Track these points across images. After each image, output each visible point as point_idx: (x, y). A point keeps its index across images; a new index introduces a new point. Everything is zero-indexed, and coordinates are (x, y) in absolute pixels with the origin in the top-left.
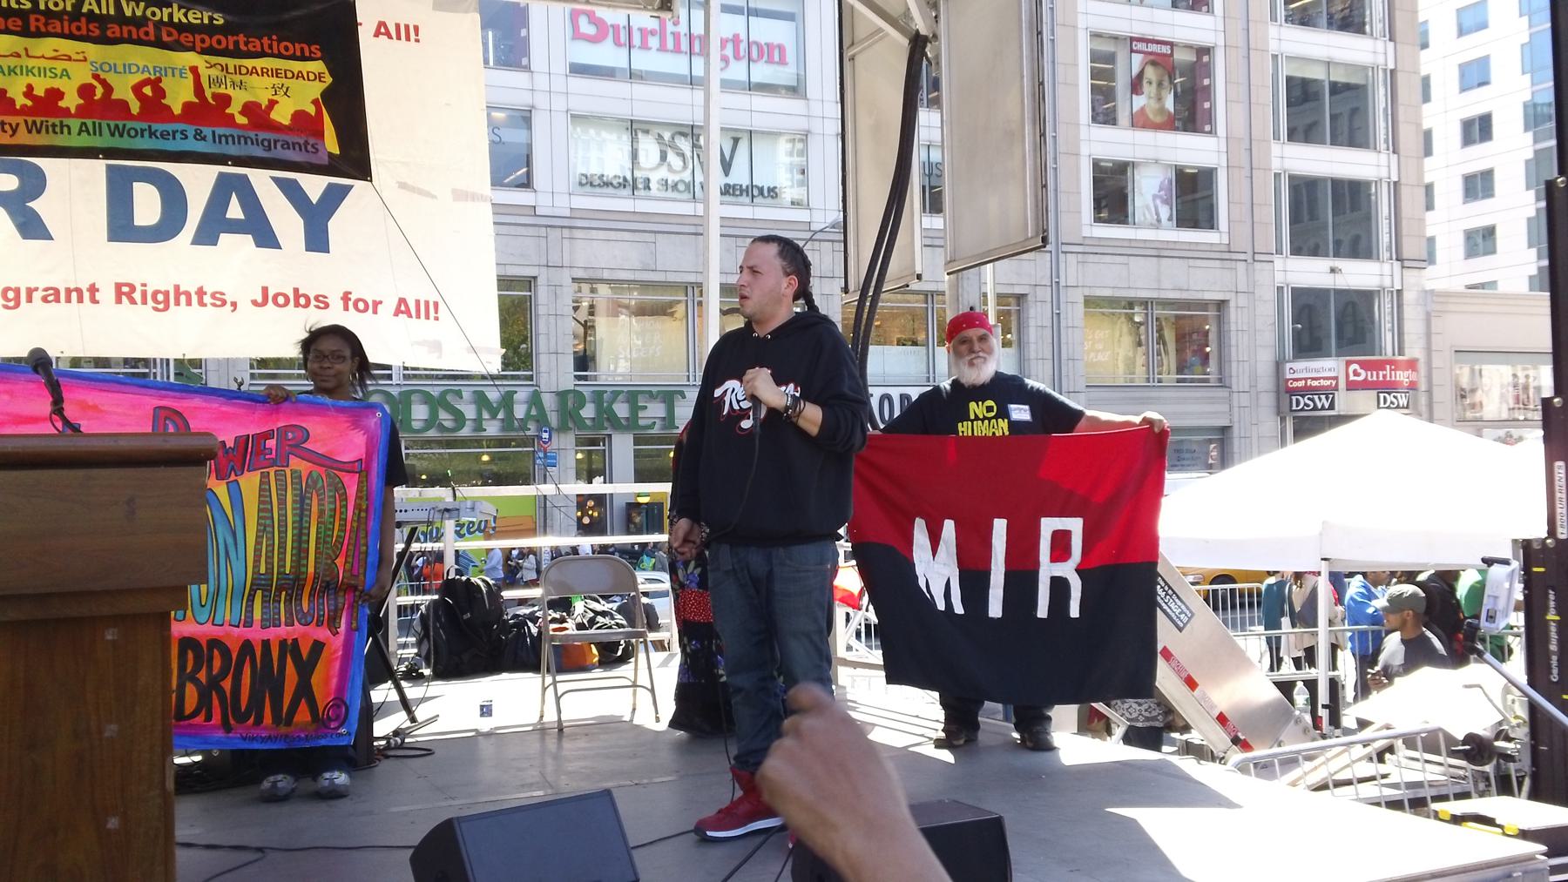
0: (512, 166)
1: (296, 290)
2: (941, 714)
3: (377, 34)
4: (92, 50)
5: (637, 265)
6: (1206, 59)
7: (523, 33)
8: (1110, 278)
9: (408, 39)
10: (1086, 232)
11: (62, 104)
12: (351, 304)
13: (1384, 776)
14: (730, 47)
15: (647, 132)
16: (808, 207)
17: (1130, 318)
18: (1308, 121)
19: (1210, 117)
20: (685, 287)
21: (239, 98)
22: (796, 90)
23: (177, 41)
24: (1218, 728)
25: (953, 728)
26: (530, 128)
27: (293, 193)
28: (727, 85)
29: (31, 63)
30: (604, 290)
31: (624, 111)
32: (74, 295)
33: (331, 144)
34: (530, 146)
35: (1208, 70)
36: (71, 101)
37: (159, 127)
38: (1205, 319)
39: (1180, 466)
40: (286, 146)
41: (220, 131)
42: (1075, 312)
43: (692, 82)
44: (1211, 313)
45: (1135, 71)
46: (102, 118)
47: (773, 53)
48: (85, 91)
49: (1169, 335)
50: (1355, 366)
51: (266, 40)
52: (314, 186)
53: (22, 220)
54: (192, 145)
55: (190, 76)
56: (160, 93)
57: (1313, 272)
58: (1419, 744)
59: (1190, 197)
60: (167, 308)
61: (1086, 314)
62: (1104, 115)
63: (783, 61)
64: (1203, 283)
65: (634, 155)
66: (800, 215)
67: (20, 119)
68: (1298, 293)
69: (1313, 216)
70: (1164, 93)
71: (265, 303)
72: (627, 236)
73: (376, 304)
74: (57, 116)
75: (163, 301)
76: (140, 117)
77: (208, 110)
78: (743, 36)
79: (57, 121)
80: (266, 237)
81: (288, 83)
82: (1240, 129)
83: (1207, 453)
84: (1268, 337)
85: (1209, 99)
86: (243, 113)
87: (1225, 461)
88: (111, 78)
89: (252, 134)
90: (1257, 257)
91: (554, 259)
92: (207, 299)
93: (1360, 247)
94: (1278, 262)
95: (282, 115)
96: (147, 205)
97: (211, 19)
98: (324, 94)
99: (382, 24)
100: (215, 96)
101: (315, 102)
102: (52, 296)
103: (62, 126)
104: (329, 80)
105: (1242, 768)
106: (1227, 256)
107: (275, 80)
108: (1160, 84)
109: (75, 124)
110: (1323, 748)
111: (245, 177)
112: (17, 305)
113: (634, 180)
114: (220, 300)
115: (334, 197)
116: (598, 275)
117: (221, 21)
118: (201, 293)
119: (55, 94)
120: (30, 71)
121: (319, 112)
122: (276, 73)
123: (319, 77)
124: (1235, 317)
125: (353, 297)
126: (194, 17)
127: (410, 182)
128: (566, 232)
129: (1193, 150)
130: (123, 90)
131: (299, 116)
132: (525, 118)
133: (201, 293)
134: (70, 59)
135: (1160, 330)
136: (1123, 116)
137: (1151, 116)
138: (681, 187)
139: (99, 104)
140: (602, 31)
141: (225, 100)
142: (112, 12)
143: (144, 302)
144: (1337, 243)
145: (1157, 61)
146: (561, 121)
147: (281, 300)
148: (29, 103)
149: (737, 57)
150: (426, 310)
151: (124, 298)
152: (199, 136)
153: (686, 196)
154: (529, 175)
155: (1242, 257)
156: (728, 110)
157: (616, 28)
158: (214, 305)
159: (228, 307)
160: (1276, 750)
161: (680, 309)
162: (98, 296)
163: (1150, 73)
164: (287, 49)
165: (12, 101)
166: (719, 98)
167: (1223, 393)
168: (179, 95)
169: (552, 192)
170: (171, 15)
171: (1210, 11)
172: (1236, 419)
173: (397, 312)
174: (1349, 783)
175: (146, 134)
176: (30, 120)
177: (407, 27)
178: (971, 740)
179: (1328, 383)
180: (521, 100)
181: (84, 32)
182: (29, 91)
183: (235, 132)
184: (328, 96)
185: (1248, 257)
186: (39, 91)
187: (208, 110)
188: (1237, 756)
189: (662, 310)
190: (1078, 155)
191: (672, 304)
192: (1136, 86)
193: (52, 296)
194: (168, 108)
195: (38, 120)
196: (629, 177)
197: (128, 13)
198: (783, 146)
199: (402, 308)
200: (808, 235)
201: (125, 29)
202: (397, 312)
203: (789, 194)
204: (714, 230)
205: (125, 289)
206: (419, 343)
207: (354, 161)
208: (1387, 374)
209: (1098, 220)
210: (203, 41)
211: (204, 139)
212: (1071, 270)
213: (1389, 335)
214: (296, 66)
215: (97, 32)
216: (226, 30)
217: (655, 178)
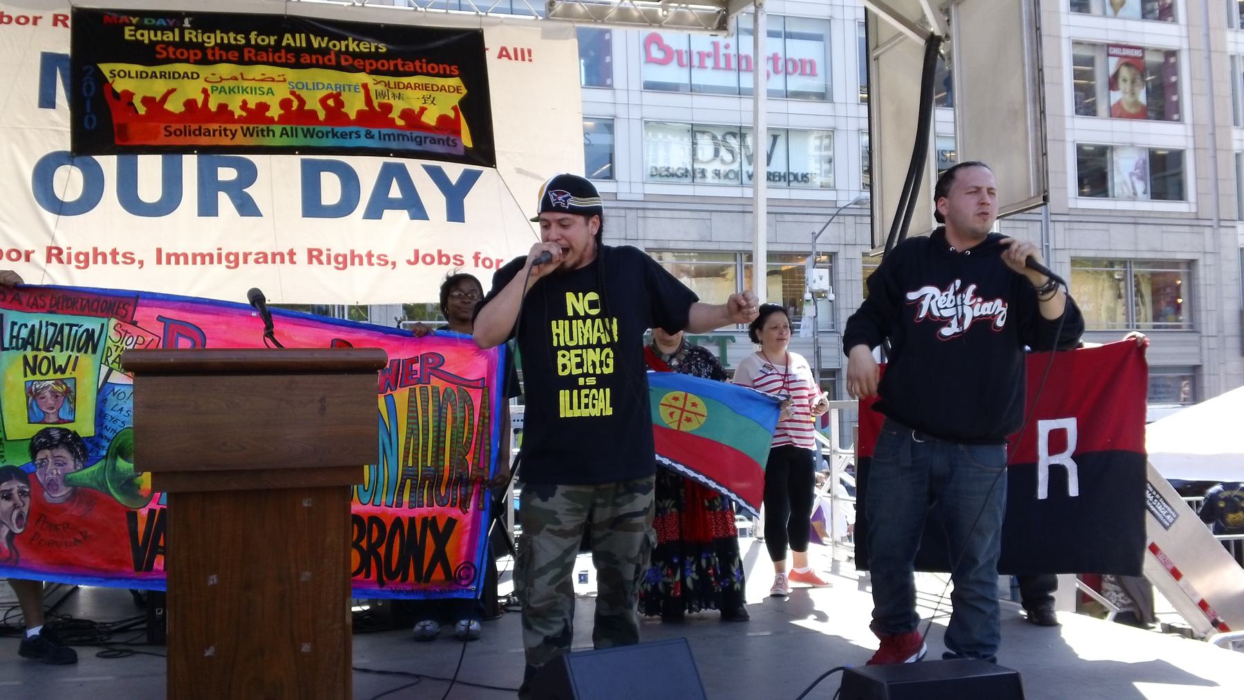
1: (439, 252)
3: (500, 56)
4: (290, 74)
5: (695, 237)
6: (1172, 60)
7: (608, 59)
8: (1092, 242)
9: (523, 59)
11: (268, 114)
12: (480, 262)
14: (771, 62)
15: (704, 132)
16: (834, 189)
17: (1111, 275)
20: (735, 254)
21: (398, 106)
22: (823, 96)
23: (352, 65)
27: (439, 177)
28: (772, 94)
29: (245, 84)
31: (687, 117)
32: (278, 258)
33: (466, 140)
34: (612, 147)
35: (1175, 69)
36: (275, 112)
38: (1177, 276)
39: (1158, 399)
40: (433, 141)
41: (385, 131)
43: (740, 92)
44: (1182, 270)
45: (1112, 71)
46: (298, 124)
47: (804, 67)
48: (285, 104)
49: (1146, 290)
51: (417, 63)
52: (454, 171)
55: (362, 91)
56: (340, 104)
59: (1160, 174)
60: (345, 267)
61: (1072, 272)
62: (1086, 107)
63: (813, 74)
64: (1173, 245)
66: (828, 195)
67: (238, 126)
70: (1137, 89)
71: (416, 261)
72: (688, 214)
74: (263, 123)
76: (326, 122)
77: (375, 116)
78: (781, 55)
79: (264, 127)
81: (434, 94)
83: (1180, 388)
87: (1196, 397)
88: (304, 94)
89: (408, 133)
92: (374, 260)
95: (430, 118)
97: (377, 48)
98: (462, 102)
99: (503, 49)
100: (381, 105)
101: (454, 108)
102: (262, 258)
103: (268, 131)
104: (464, 91)
107: (425, 93)
108: (1133, 82)
109: (278, 129)
111: (402, 167)
112: (237, 265)
113: (694, 170)
115: (468, 180)
116: (666, 245)
117: (384, 50)
118: (370, 255)
119: (263, 107)
120: (244, 90)
122: (426, 87)
123: (457, 90)
125: (482, 256)
126: (364, 47)
127: (525, 168)
128: (640, 213)
129: (1163, 135)
130: (313, 102)
131: (443, 119)
132: (608, 126)
133: (370, 255)
134: (273, 80)
135: (1138, 285)
136: (1102, 108)
137: (1126, 108)
138: (731, 176)
139: (296, 114)
140: (669, 55)
141: (388, 108)
142: (304, 45)
143: (329, 263)
145: (1130, 63)
146: (637, 127)
147: (428, 259)
148: (244, 114)
149: (776, 71)
151: (314, 260)
152: (369, 136)
153: (736, 182)
154: (611, 170)
156: (772, 113)
157: (679, 53)
161: (731, 272)
162: (295, 258)
163: (1125, 73)
164: (433, 69)
165: (232, 113)
166: (765, 105)
167: (1194, 337)
168: (354, 105)
170: (347, 46)
171: (1175, 21)
172: (1205, 358)
176: (245, 127)
177: (522, 51)
180: (605, 111)
181: (283, 60)
182: (244, 106)
183: (396, 132)
184: (465, 105)
186: (252, 105)
187: (375, 116)
190: (1063, 141)
191: (723, 268)
192: (1113, 83)
193: (262, 258)
194: (346, 115)
196: (690, 168)
197: (316, 45)
198: (813, 142)
201: (314, 57)
203: (817, 181)
204: (762, 209)
205: (315, 253)
207: (483, 153)
210: (371, 65)
211: (372, 137)
212: (1059, 235)
214: (440, 81)
215: (293, 60)
216: (388, 56)
217: (710, 169)
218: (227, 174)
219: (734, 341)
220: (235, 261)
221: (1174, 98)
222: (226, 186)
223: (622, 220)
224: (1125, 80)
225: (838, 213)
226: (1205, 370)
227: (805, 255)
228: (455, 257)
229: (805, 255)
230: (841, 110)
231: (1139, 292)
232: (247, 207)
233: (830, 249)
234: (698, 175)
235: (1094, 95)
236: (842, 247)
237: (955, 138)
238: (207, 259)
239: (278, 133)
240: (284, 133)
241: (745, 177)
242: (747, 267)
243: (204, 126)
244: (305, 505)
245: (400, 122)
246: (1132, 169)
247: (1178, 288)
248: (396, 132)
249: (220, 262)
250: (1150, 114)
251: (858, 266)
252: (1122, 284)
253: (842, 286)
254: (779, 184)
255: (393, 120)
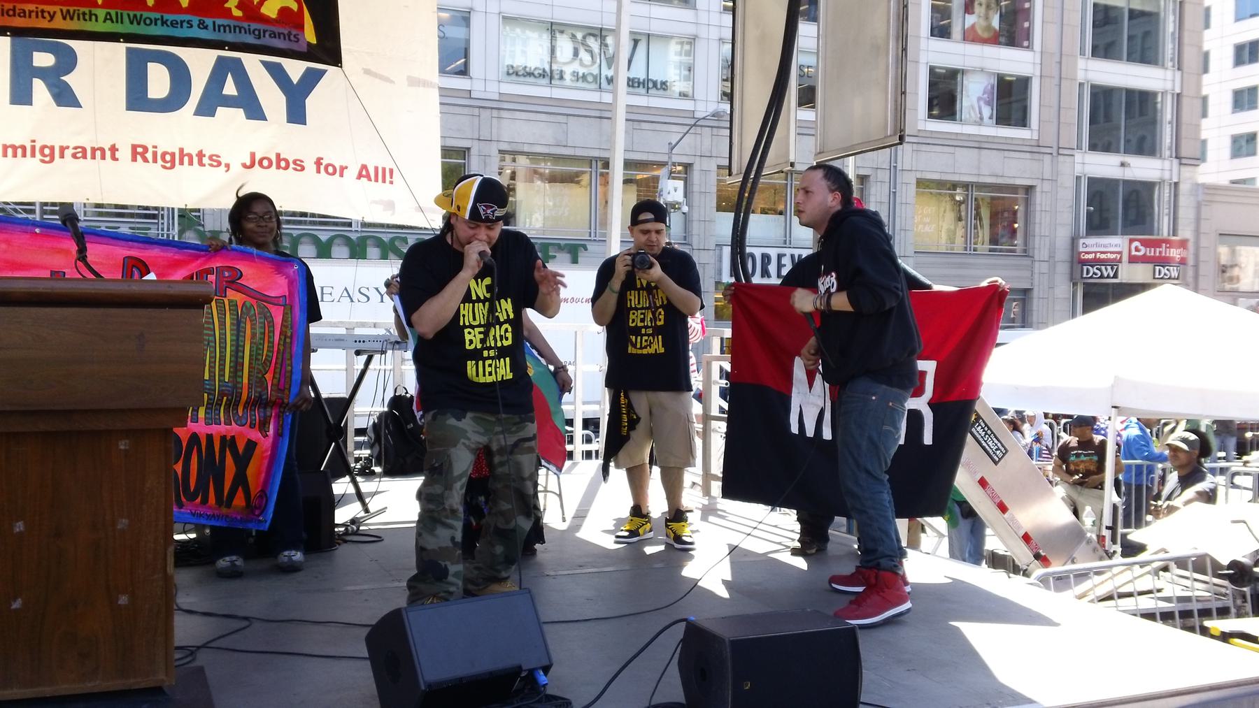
0: (456, 59)
1: (278, 155)
2: (797, 527)
5: (551, 141)
8: (938, 165)
10: (921, 126)
13: (1159, 591)
15: (562, 32)
18: (1109, 40)
19: (1028, 35)
20: (590, 161)
24: (1022, 544)
25: (807, 539)
26: (468, 26)
27: (278, 74)
30: (523, 161)
32: (98, 153)
34: (468, 41)
37: (169, 17)
38: (1015, 201)
40: (273, 35)
41: (219, 21)
42: (908, 191)
44: (1021, 196)
46: (126, 9)
49: (985, 213)
50: (1136, 244)
52: (295, 69)
53: (56, 90)
54: (196, 33)
57: (1106, 165)
58: (1190, 566)
59: (1006, 100)
60: (173, 166)
61: (917, 193)
62: (941, 31)
64: (1015, 171)
65: (553, 51)
68: (1092, 181)
69: (1108, 117)
72: (543, 117)
73: (343, 169)
75: (171, 160)
79: (87, 10)
80: (255, 111)
82: (1053, 46)
84: (1066, 217)
85: (1028, 19)
86: (238, 7)
89: (245, 25)
90: (1061, 151)
91: (485, 134)
92: (206, 160)
93: (1145, 146)
94: (1078, 157)
96: (158, 81)
103: (91, 15)
105: (1044, 581)
106: (1035, 149)
109: (101, 13)
110: (1110, 567)
111: (239, 60)
113: (551, 71)
114: (216, 161)
115: (311, 79)
118: (201, 155)
121: (300, 8)
124: (1039, 199)
128: (495, 113)
129: (1012, 61)
131: (284, 11)
132: (464, 18)
133: (201, 155)
135: (978, 208)
136: (957, 31)
137: (980, 32)
138: (590, 79)
143: (155, 161)
144: (1127, 141)
146: (494, 21)
147: (265, 163)
150: (383, 175)
151: (139, 157)
152: (203, 26)
153: (594, 86)
154: (466, 64)
155: (1048, 150)
158: (211, 165)
159: (223, 168)
160: (1069, 567)
161: (585, 179)
162: (117, 155)
167: (1026, 261)
169: (485, 79)
172: (1036, 282)
173: (360, 176)
174: (1130, 595)
175: (159, 22)
176: (65, 9)
178: (822, 549)
179: (1113, 256)
183: (232, 23)
185: (1054, 151)
188: (1039, 571)
189: (571, 179)
191: (578, 174)
195: (71, 9)
196: (547, 69)
198: (674, 47)
199: (363, 173)
200: (693, 121)
202: (360, 176)
203: (678, 86)
204: (621, 115)
205: (140, 150)
206: (376, 202)
208: (1163, 251)
209: (930, 116)
211: (206, 28)
213: (1166, 219)
217: (568, 70)
218: (43, 59)
219: (586, 249)
220: (49, 154)
221: (1026, 25)
222: (42, 73)
223: (476, 119)
224: (981, 4)
225: (695, 124)
226: (1035, 293)
227: (662, 164)
228: (295, 162)
229: (662, 164)
230: (703, 18)
231: (978, 216)
232: (65, 97)
233: (685, 160)
234: (557, 77)
235: (949, 17)
236: (698, 159)
237: (818, 53)
238: (20, 151)
239: (101, 18)
240: (108, 18)
241: (604, 81)
242: (602, 174)
243: (19, 6)
244: (122, 447)
245: (237, 13)
246: (980, 94)
247: (1015, 213)
248: (232, 23)
249: (33, 155)
250: (1002, 39)
251: (713, 178)
252: (963, 207)
253: (696, 198)
254: (637, 90)
255: (230, 10)
